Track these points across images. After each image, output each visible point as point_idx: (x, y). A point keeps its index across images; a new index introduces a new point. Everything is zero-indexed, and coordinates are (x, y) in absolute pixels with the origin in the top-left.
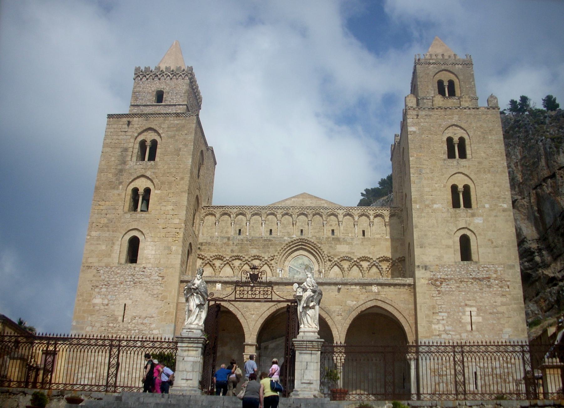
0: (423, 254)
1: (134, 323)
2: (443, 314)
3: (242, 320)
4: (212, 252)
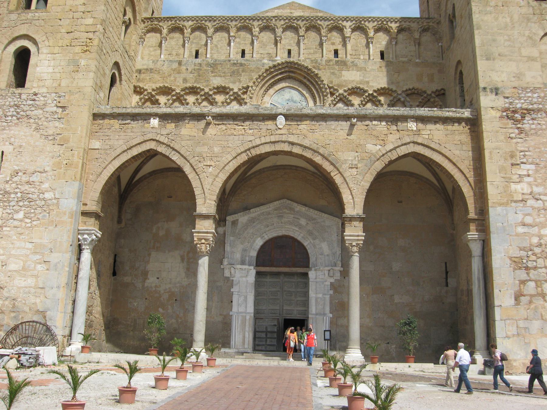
0: (492, 70)
1: (16, 182)
2: (528, 166)
3: (191, 176)
4: (155, 83)
